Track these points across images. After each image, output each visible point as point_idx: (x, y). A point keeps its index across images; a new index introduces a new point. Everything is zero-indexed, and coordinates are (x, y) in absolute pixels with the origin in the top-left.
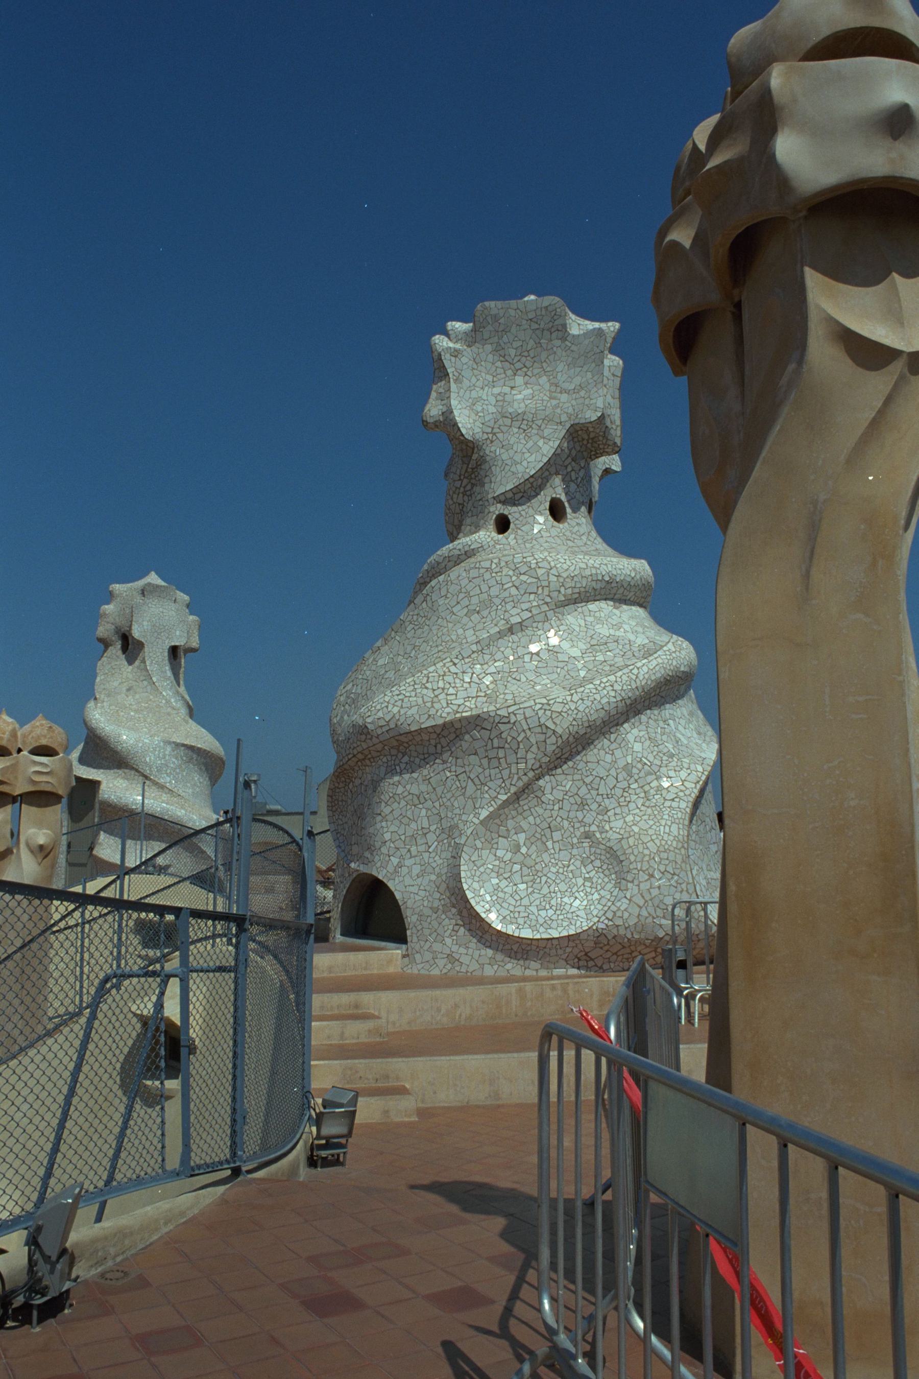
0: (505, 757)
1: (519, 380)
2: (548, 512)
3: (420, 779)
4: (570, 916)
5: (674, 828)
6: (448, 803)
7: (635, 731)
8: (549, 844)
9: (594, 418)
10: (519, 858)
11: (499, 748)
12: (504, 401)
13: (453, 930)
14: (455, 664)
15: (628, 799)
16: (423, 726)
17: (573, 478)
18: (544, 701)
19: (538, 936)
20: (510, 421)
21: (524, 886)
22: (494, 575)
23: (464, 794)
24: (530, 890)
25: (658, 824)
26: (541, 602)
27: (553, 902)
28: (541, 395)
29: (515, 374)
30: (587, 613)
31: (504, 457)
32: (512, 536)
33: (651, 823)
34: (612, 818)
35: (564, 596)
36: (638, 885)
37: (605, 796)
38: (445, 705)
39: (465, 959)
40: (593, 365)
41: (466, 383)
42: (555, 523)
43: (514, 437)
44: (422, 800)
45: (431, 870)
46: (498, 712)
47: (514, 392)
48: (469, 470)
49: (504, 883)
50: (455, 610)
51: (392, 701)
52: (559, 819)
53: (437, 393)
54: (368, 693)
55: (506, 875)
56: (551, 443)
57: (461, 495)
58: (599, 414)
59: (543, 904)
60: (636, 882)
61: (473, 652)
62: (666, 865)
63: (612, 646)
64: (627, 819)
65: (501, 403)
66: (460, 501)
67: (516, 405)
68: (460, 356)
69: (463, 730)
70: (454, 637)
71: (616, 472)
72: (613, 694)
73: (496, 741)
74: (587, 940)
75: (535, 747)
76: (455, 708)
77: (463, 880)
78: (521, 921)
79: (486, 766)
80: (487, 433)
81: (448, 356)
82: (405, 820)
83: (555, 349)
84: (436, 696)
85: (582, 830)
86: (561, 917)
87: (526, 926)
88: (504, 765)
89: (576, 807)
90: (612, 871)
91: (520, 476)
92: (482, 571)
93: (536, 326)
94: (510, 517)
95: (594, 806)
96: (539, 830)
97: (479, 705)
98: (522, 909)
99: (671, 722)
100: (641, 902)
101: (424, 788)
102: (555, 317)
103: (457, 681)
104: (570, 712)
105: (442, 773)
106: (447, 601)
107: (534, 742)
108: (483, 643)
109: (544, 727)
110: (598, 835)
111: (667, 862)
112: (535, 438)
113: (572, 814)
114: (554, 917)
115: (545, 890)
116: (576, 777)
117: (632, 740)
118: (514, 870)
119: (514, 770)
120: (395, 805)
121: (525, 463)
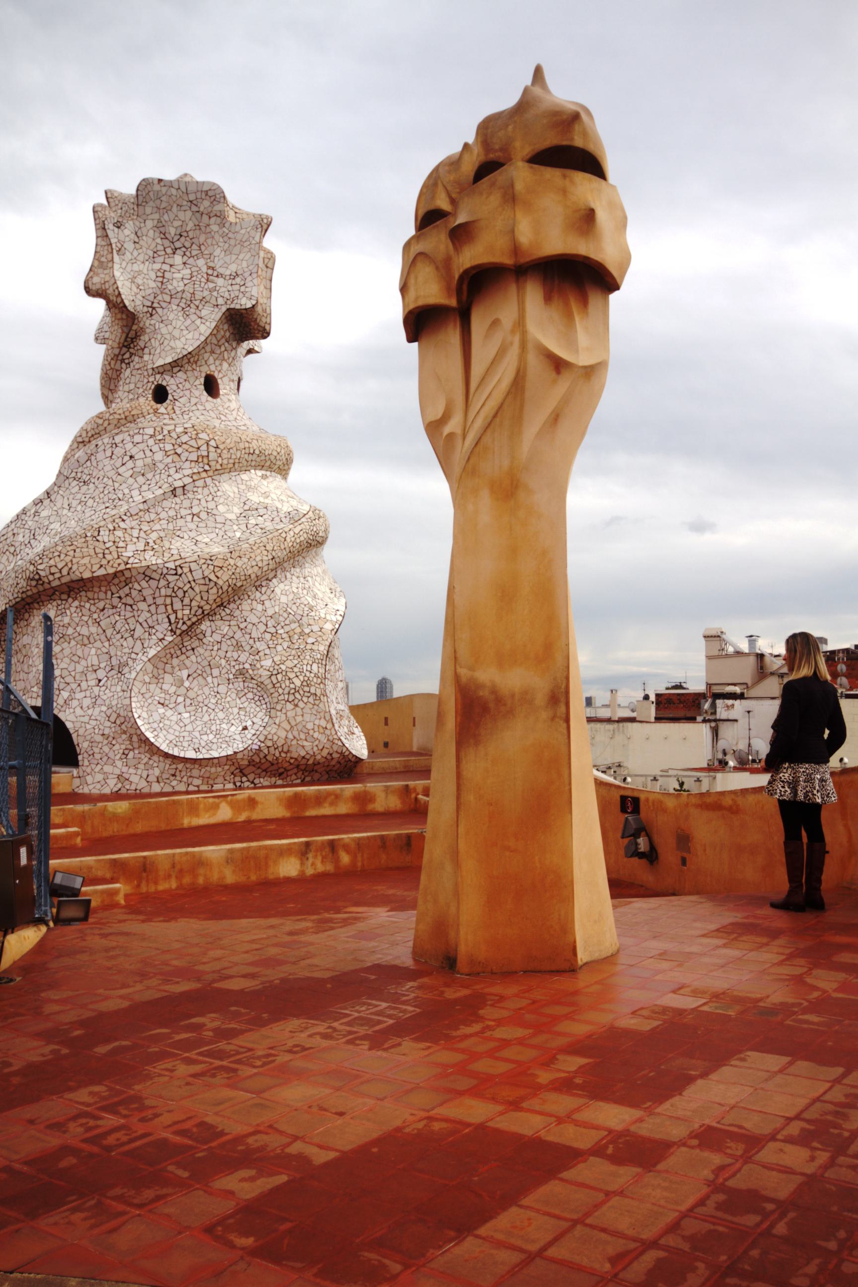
0: (172, 604)
1: (178, 259)
2: (202, 387)
3: (90, 622)
4: (227, 739)
5: (315, 666)
6: (118, 644)
7: (282, 586)
8: (209, 679)
9: (249, 305)
10: (182, 691)
11: (166, 596)
12: (163, 277)
13: (124, 754)
14: (123, 520)
15: (275, 642)
16: (95, 575)
17: (226, 357)
18: (208, 557)
19: (201, 757)
21: (187, 715)
23: (132, 636)
24: (193, 718)
27: (214, 728)
28: (199, 276)
29: (174, 253)
30: (239, 481)
31: (164, 330)
32: (170, 407)
33: (296, 662)
34: (263, 658)
38: (116, 557)
39: (135, 779)
40: (249, 255)
41: (128, 256)
42: (210, 398)
43: (173, 314)
44: (92, 641)
45: (102, 702)
46: (166, 565)
47: (173, 270)
49: (169, 713)
50: (121, 470)
51: (64, 551)
52: (217, 658)
54: (32, 541)
55: (171, 706)
56: (208, 324)
57: (119, 362)
58: (254, 302)
59: (205, 729)
60: (284, 711)
61: (141, 510)
64: (275, 659)
65: (161, 279)
66: (118, 367)
67: (175, 283)
68: (122, 227)
69: (133, 579)
70: (121, 496)
72: (265, 553)
73: (163, 592)
74: (242, 759)
75: (199, 596)
76: (125, 559)
77: (134, 710)
78: (185, 744)
79: (153, 611)
81: (111, 226)
82: (76, 659)
84: (107, 549)
85: (237, 667)
86: (220, 740)
87: (190, 748)
88: (170, 611)
89: (231, 648)
90: (263, 702)
91: (178, 351)
92: (146, 437)
93: (197, 209)
94: (168, 388)
95: (247, 648)
96: (200, 667)
97: (147, 557)
98: (186, 734)
99: (309, 579)
100: (288, 727)
101: (94, 629)
102: (215, 203)
103: (126, 535)
104: (230, 567)
105: (112, 617)
106: (112, 462)
107: (198, 591)
108: (150, 503)
109: (207, 579)
110: (250, 672)
112: (193, 317)
113: (229, 655)
114: (215, 741)
115: (206, 718)
116: (232, 623)
117: (279, 593)
118: (178, 701)
119: (180, 615)
120: (66, 645)
121: (183, 340)
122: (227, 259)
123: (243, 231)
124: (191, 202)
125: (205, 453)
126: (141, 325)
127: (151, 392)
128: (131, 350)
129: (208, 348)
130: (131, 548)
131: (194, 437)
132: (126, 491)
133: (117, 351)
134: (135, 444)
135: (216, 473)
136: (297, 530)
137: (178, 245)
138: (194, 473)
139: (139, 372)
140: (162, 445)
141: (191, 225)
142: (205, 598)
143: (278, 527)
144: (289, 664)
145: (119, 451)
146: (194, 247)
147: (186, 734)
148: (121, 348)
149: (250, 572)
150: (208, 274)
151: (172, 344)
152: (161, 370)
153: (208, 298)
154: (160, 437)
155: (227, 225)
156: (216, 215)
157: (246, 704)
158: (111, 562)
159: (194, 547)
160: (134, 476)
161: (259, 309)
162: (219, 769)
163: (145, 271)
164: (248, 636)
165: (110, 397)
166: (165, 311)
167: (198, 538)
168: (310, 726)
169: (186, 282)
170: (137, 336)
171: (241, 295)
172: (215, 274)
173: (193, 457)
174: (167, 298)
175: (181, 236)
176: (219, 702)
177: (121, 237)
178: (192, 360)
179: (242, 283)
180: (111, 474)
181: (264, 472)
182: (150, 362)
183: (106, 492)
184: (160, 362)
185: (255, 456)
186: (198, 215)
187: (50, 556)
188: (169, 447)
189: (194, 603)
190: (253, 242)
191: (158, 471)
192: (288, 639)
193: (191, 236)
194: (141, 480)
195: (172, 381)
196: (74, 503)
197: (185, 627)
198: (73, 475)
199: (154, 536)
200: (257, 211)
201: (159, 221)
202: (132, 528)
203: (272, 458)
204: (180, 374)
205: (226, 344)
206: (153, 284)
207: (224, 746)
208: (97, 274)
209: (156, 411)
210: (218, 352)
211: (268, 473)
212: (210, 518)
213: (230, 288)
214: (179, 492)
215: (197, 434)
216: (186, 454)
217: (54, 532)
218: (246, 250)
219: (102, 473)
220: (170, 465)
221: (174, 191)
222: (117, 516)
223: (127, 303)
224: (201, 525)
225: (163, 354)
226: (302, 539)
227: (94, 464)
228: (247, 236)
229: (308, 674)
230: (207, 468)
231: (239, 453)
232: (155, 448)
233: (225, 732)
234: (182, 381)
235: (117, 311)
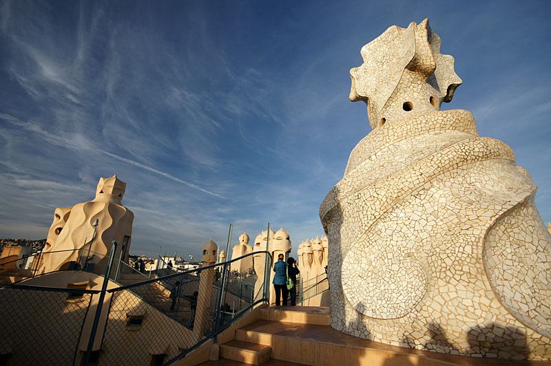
4: (395, 305)
5: (468, 249)
7: (441, 192)
8: (386, 261)
25: (454, 246)
27: (386, 296)
33: (449, 245)
36: (438, 289)
37: (419, 231)
49: (363, 282)
52: (391, 246)
59: (381, 296)
60: (436, 286)
62: (461, 275)
71: (458, 85)
85: (406, 252)
98: (369, 298)
100: (442, 302)
110: (415, 254)
111: (462, 273)
113: (399, 243)
114: (386, 305)
115: (382, 288)
117: (438, 197)
142: (374, 208)
144: (443, 247)
147: (369, 298)
149: (402, 186)
157: (412, 279)
162: (392, 329)
164: (412, 230)
168: (468, 302)
176: (392, 277)
185: (423, 125)
189: (369, 213)
192: (447, 228)
197: (367, 228)
207: (391, 311)
229: (460, 255)
233: (395, 300)
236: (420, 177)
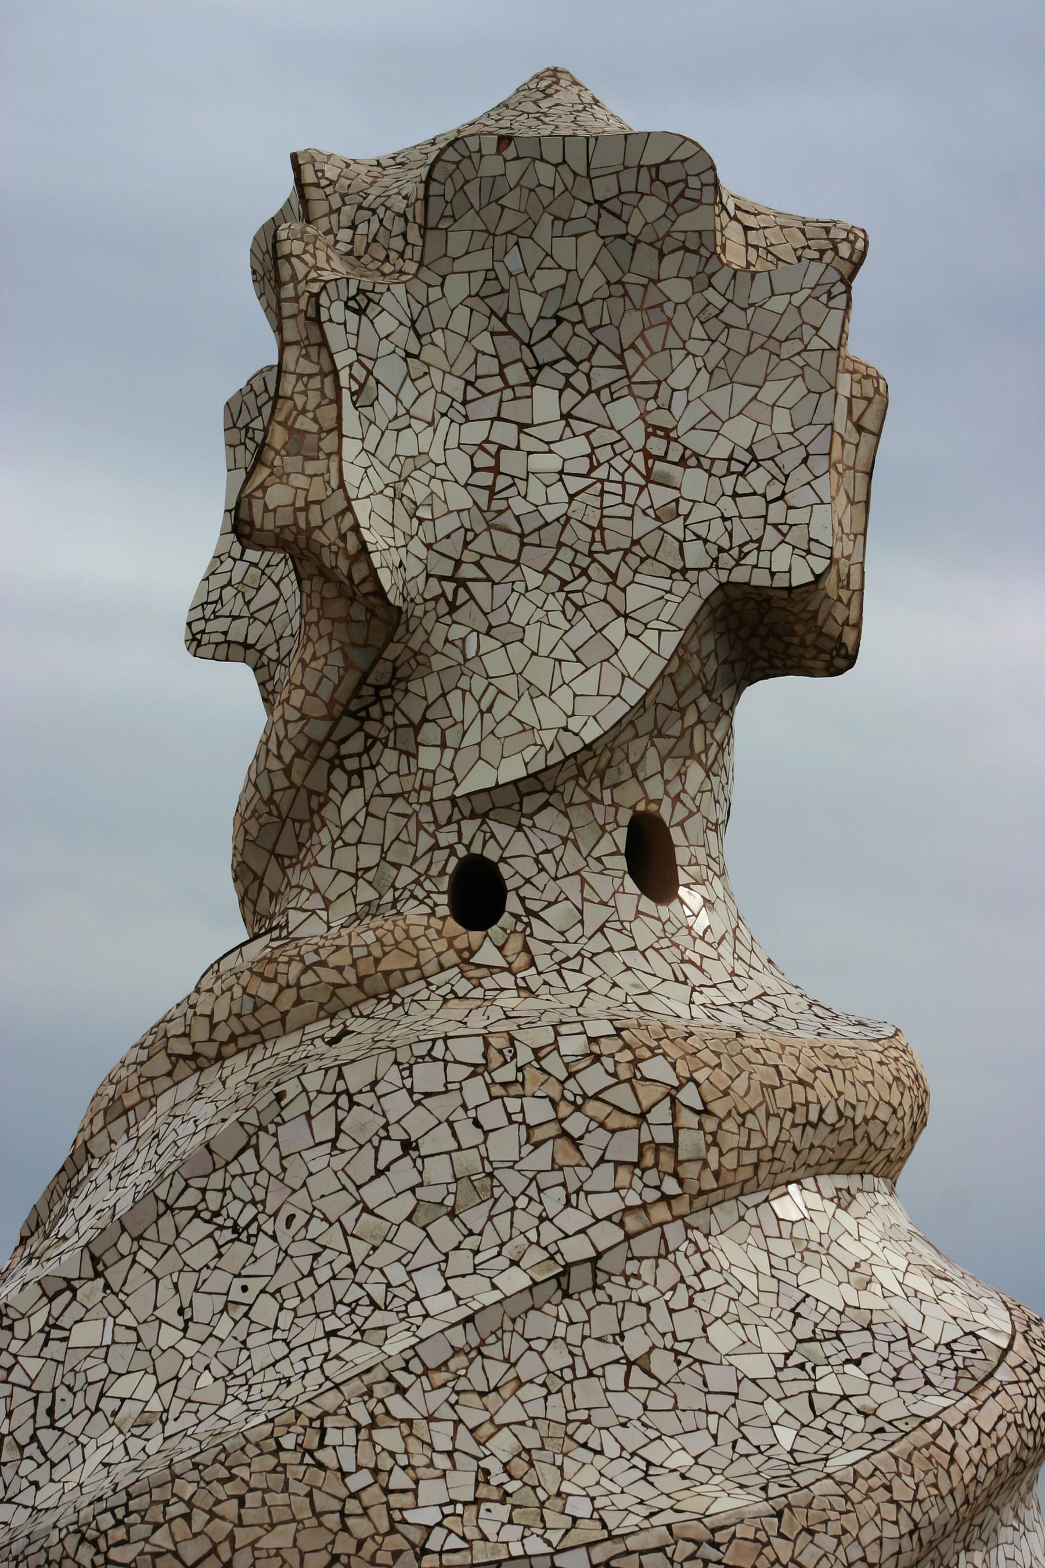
1: (545, 403)
2: (621, 863)
9: (801, 576)
12: (496, 470)
17: (698, 746)
18: (700, 1531)
20: (515, 541)
22: (497, 1090)
26: (651, 1195)
28: (619, 464)
29: (533, 382)
30: (771, 1229)
31: (496, 663)
32: (515, 944)
35: (717, 1175)
38: (384, 1526)
42: (647, 904)
43: (529, 603)
47: (527, 443)
48: (367, 691)
50: (373, 1194)
51: (204, 1500)
53: (291, 430)
54: (47, 1437)
56: (650, 638)
58: (820, 566)
63: (857, 1343)
65: (486, 479)
66: (317, 782)
67: (536, 492)
70: (378, 1293)
80: (441, 578)
81: (338, 311)
83: (669, 307)
84: (355, 1495)
91: (548, 738)
92: (457, 1072)
93: (619, 228)
94: (505, 870)
97: (490, 1529)
106: (339, 1162)
108: (487, 1322)
112: (599, 614)
121: (563, 696)
122: (719, 400)
123: (778, 304)
124: (600, 204)
125: (665, 1135)
126: (415, 643)
127: (445, 883)
128: (371, 727)
129: (645, 724)
130: (431, 1492)
131: (624, 1073)
132: (396, 1273)
133: (319, 730)
134: (420, 1099)
135: (699, 1202)
136: (986, 1419)
137: (547, 351)
138: (628, 1209)
139: (400, 806)
140: (513, 1105)
141: (594, 281)
143: (925, 1410)
145: (361, 1122)
146: (602, 356)
148: (336, 721)
150: (647, 455)
151: (524, 711)
152: (482, 804)
153: (650, 544)
154: (507, 1073)
155: (721, 280)
156: (684, 248)
158: (369, 1547)
159: (643, 1490)
160: (421, 1218)
161: (830, 584)
163: (437, 455)
165: (273, 878)
166: (501, 591)
167: (655, 1453)
169: (575, 484)
170: (397, 680)
171: (771, 537)
172: (674, 455)
173: (625, 1147)
174: (508, 546)
175: (560, 321)
177: (368, 346)
178: (588, 769)
179: (774, 491)
180: (336, 1205)
181: (842, 1181)
182: (443, 775)
183: (323, 1274)
184: (480, 778)
186: (622, 248)
187: (156, 1514)
188: (538, 1111)
190: (816, 343)
191: (506, 1202)
193: (592, 321)
194: (445, 1231)
195: (519, 844)
196: (204, 1307)
198: (191, 1197)
199: (503, 1444)
200: (818, 211)
201: (490, 275)
202: (430, 1418)
203: (875, 1129)
204: (544, 819)
205: (704, 702)
206: (460, 499)
208: (283, 477)
209: (466, 958)
210: (675, 730)
211: (854, 1182)
212: (686, 1375)
213: (728, 507)
214: (581, 1277)
215: (635, 1063)
216: (601, 1137)
217: (131, 1409)
218: (788, 369)
219: (301, 1198)
220: (544, 1180)
221: (545, 174)
222: (380, 1374)
223: (385, 578)
224: (656, 1401)
225: (491, 748)
226: (1004, 1449)
227: (272, 1163)
228: (791, 321)
230: (671, 1186)
231: (774, 1122)
232: (492, 1115)
234: (552, 842)
235: (330, 591)
236: (906, 1540)
